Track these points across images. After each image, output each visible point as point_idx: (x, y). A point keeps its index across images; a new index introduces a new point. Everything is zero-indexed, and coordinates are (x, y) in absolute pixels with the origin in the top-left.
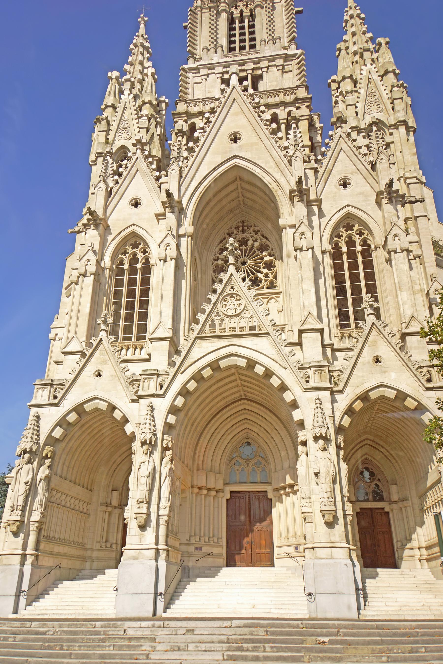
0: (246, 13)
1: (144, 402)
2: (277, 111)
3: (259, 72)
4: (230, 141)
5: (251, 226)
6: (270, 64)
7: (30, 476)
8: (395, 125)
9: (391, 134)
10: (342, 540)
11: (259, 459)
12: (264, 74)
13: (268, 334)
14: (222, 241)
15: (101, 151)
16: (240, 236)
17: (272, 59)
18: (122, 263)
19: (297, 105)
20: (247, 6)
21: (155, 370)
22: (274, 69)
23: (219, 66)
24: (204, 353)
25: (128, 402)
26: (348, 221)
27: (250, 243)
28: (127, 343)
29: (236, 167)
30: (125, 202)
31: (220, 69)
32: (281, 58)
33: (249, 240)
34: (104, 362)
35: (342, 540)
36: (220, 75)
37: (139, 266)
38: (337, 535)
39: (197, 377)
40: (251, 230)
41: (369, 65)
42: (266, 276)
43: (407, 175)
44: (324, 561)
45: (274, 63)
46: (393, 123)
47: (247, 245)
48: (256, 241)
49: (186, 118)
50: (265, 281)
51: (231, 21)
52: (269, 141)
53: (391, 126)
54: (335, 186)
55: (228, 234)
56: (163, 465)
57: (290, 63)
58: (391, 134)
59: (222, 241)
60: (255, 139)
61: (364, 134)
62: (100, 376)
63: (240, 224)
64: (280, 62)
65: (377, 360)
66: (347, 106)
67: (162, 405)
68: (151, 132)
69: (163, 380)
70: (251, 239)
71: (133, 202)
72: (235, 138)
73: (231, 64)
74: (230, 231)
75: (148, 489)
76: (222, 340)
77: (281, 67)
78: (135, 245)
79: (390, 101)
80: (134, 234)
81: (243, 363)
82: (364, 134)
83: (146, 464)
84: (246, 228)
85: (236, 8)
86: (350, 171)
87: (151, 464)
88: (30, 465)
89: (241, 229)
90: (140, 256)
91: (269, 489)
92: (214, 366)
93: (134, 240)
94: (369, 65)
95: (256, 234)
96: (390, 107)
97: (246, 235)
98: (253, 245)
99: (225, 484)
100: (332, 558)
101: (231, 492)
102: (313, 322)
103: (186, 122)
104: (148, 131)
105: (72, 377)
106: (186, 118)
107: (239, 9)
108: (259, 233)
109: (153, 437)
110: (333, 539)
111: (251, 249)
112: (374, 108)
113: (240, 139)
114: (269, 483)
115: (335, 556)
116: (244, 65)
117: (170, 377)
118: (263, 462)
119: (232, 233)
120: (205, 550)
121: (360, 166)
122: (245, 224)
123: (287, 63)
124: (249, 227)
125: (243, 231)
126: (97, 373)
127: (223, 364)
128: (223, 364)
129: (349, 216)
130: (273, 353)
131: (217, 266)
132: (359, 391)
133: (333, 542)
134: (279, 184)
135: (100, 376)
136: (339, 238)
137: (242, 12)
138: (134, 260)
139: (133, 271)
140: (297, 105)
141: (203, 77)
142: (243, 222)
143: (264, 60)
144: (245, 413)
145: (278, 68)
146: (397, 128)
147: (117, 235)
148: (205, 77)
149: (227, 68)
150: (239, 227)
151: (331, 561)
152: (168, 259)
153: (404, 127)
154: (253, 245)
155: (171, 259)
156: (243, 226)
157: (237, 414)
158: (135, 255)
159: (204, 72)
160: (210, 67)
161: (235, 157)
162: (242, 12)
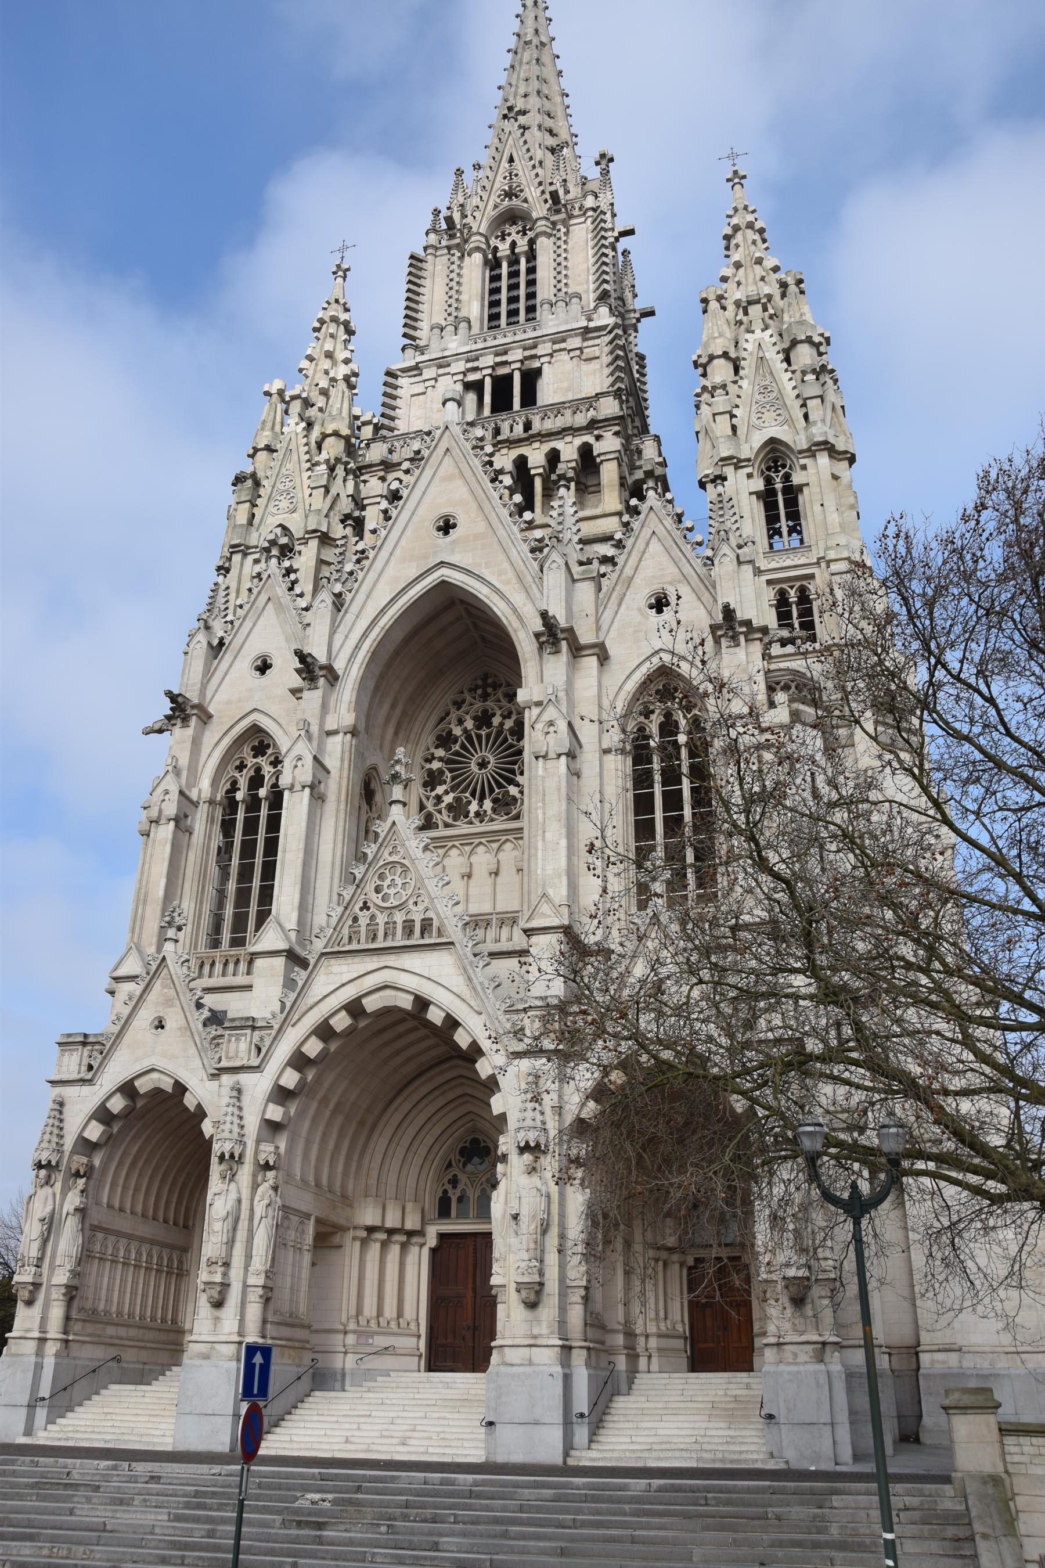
0: (522, 245)
1: (227, 1079)
2: (559, 445)
3: (536, 364)
4: (436, 533)
5: (500, 685)
6: (557, 347)
7: (49, 1208)
8: (809, 450)
9: (804, 467)
10: (552, 1333)
12: (546, 369)
13: (452, 943)
14: (442, 719)
15: (237, 542)
16: (478, 705)
17: (559, 338)
18: (234, 787)
19: (596, 432)
20: (525, 234)
21: (247, 1019)
22: (564, 356)
23: (457, 360)
24: (334, 986)
25: (205, 1078)
26: (664, 685)
27: (496, 721)
28: (234, 951)
29: (444, 585)
30: (244, 665)
31: (460, 366)
32: (576, 335)
33: (494, 715)
34: (168, 1003)
35: (552, 1333)
36: (461, 377)
37: (262, 792)
38: (544, 1324)
39: (324, 1031)
41: (758, 331)
44: (515, 1369)
45: (563, 345)
46: (805, 447)
47: (489, 725)
49: (382, 473)
51: (493, 264)
52: (510, 528)
53: (800, 452)
54: (639, 610)
56: (257, 1198)
57: (596, 342)
58: (804, 467)
59: (442, 719)
60: (481, 527)
61: (749, 470)
62: (162, 1027)
63: (480, 682)
64: (575, 342)
66: (714, 415)
67: (258, 1087)
68: (333, 491)
69: (262, 1039)
70: (499, 713)
71: (259, 663)
72: (446, 526)
73: (482, 355)
75: (225, 1240)
76: (367, 959)
77: (578, 352)
78: (260, 750)
79: (800, 402)
80: (256, 730)
81: (406, 1002)
82: (749, 470)
83: (223, 1197)
85: (503, 239)
86: (669, 579)
87: (233, 1196)
88: (48, 1190)
89: (479, 691)
90: (267, 770)
92: (354, 1008)
93: (257, 740)
94: (758, 331)
96: (799, 414)
97: (490, 704)
98: (502, 724)
100: (531, 1363)
101: (442, 1236)
102: (549, 912)
104: (327, 491)
105: (116, 1029)
106: (382, 473)
107: (509, 240)
109: (237, 1147)
110: (535, 1332)
111: (500, 732)
112: (769, 416)
113: (454, 526)
115: (535, 1360)
116: (506, 353)
117: (274, 1032)
119: (464, 701)
120: (381, 1341)
121: (687, 569)
122: (490, 681)
123: (591, 343)
124: (496, 686)
125: (485, 697)
126: (156, 1023)
127: (371, 1004)
128: (371, 1004)
129: (664, 672)
130: (457, 982)
131: (430, 772)
133: (535, 1337)
134: (519, 617)
135: (162, 1027)
136: (647, 717)
137: (513, 244)
138: (257, 781)
139: (254, 804)
140: (596, 432)
141: (427, 384)
142: (485, 677)
143: (544, 342)
144: (462, 1084)
145: (572, 354)
146: (814, 456)
147: (225, 734)
148: (432, 383)
149: (473, 361)
150: (477, 687)
151: (528, 1370)
152: (298, 787)
153: (825, 454)
154: (502, 724)
155: (304, 787)
156: (485, 686)
157: (447, 1087)
158: (258, 769)
159: (429, 373)
160: (442, 363)
162: (513, 244)
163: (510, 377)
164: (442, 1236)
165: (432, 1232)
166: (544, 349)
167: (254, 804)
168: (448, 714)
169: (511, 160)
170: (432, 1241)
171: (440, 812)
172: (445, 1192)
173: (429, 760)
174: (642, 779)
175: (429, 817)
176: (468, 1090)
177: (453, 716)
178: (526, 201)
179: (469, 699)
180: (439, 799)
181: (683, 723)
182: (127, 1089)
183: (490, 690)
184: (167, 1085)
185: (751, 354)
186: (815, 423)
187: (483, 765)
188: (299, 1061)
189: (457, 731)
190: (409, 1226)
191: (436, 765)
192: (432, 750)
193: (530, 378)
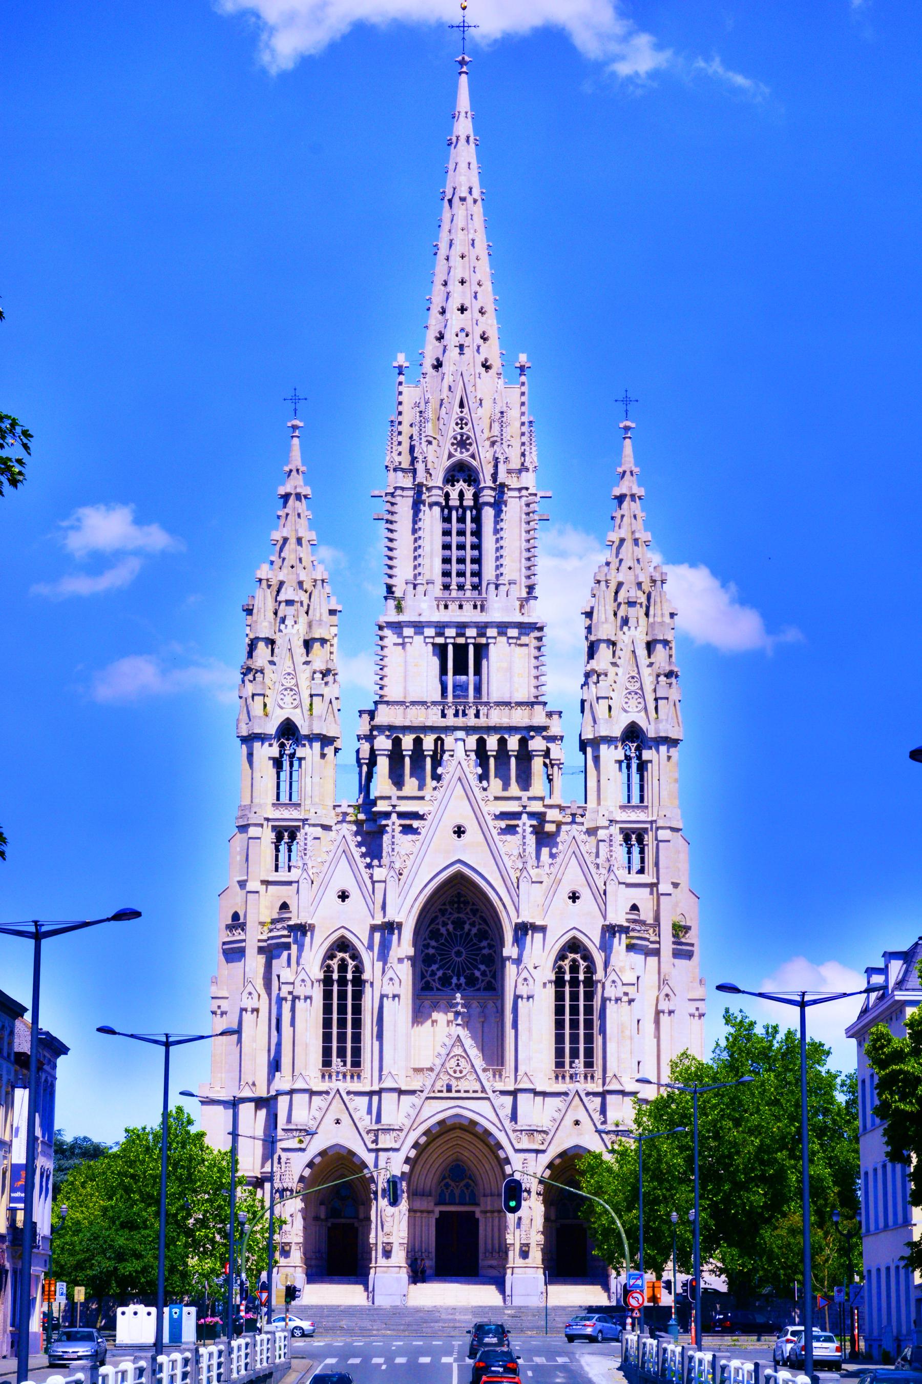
11: (470, 1181)
12: (491, 647)
17: (502, 628)
27: (467, 927)
40: (468, 910)
42: (484, 974)
43: (660, 823)
48: (473, 924)
50: (483, 981)
55: (440, 910)
65: (577, 1123)
72: (459, 831)
74: (443, 907)
84: (462, 905)
89: (456, 905)
91: (477, 1211)
95: (474, 915)
99: (437, 1204)
101: (440, 1212)
103: (388, 737)
108: (478, 916)
112: (633, 702)
114: (477, 1204)
118: (472, 1184)
131: (427, 955)
132: (560, 1149)
137: (461, 495)
139: (342, 981)
160: (419, 627)
161: (459, 861)
162: (461, 495)
163: (466, 645)
164: (440, 1212)
165: (438, 1209)
166: (492, 632)
167: (342, 981)
168: (436, 917)
169: (462, 405)
170: (437, 1215)
171: (434, 980)
172: (442, 1191)
173: (427, 946)
174: (559, 996)
175: (427, 983)
176: (459, 1142)
177: (440, 920)
178: (473, 456)
179: (450, 910)
180: (433, 974)
181: (582, 968)
182: (322, 1154)
183: (462, 905)
184: (344, 1153)
185: (626, 646)
186: (662, 721)
187: (458, 954)
188: (416, 1145)
189: (443, 930)
190: (430, 1209)
191: (431, 951)
192: (429, 941)
193: (481, 651)
